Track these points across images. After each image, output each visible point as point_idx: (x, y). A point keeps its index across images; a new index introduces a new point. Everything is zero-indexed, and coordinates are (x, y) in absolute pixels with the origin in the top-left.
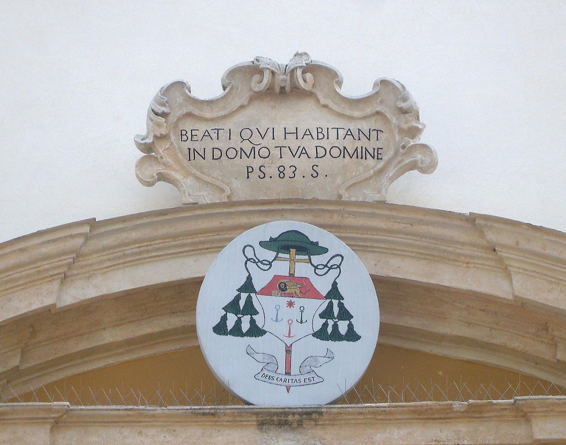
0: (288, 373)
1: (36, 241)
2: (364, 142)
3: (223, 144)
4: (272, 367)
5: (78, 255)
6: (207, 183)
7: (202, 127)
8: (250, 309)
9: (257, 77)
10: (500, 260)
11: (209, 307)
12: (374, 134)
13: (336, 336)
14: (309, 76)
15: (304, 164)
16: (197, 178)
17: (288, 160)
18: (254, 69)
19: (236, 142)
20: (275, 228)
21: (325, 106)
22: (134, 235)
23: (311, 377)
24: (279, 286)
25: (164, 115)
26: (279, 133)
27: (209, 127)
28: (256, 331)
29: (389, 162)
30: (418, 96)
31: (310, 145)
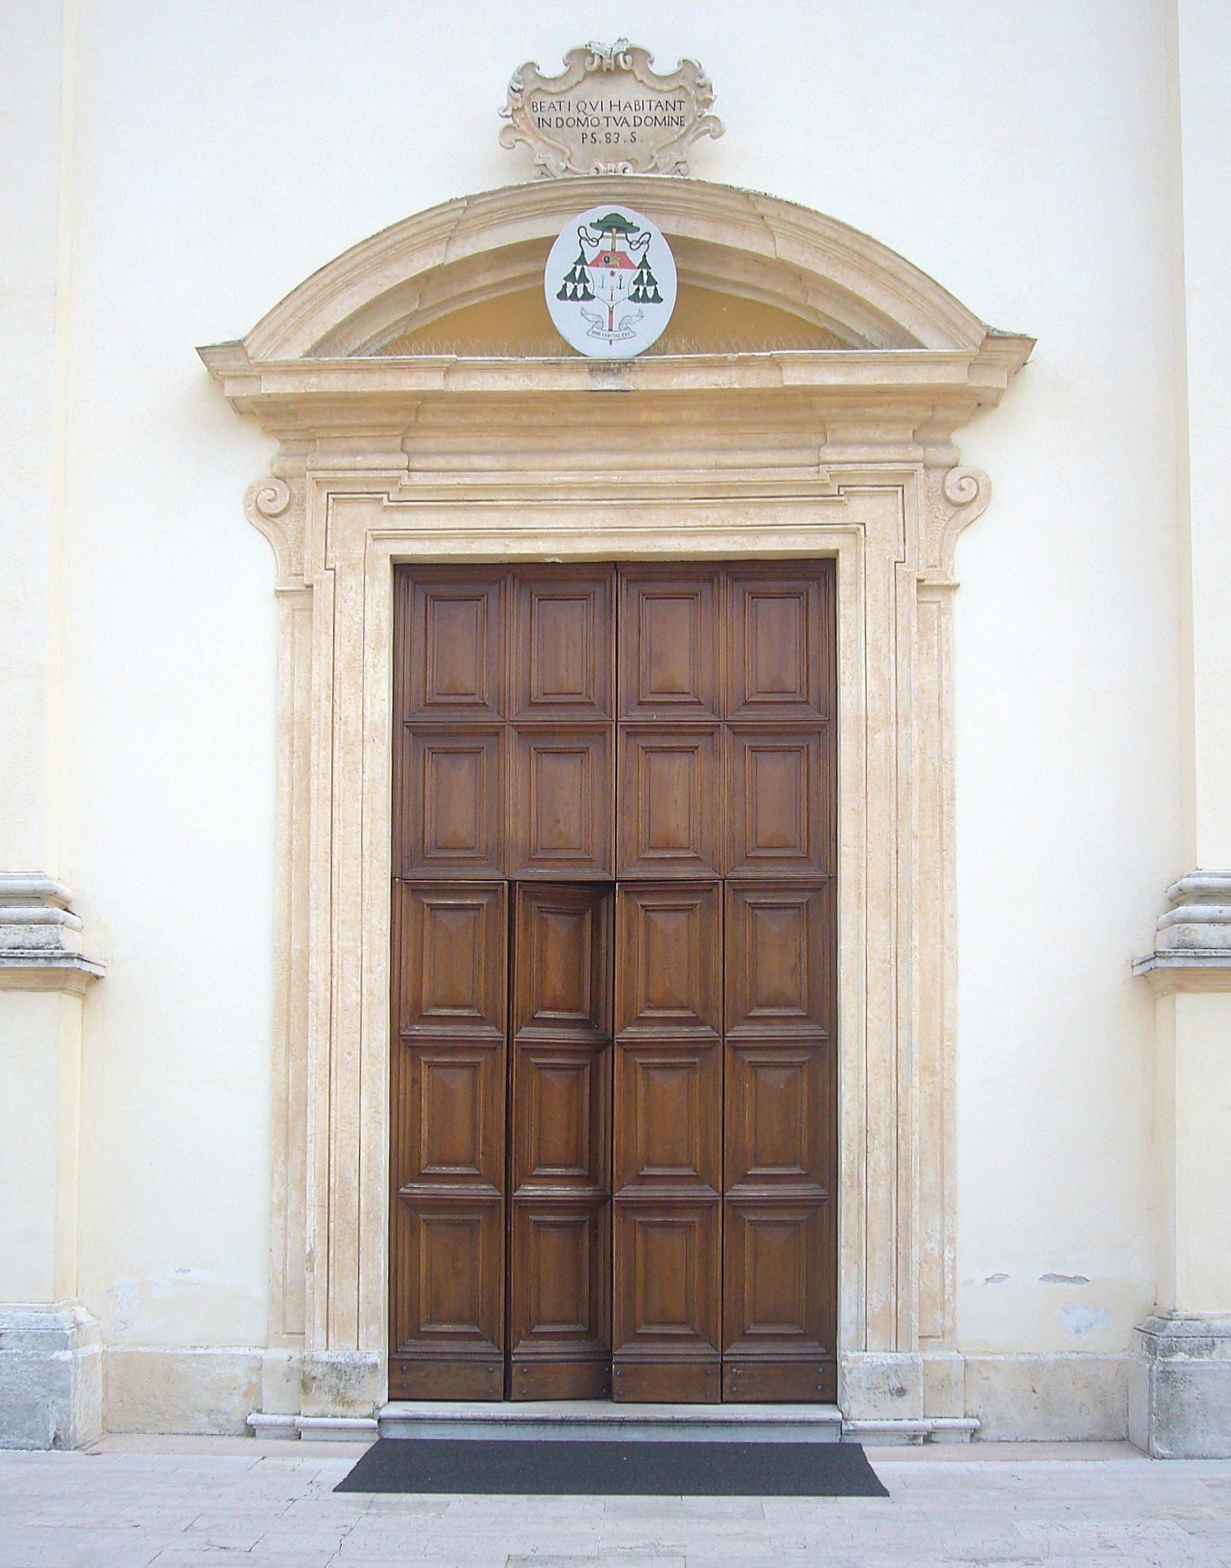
0: (611, 330)
1: (429, 215)
2: (670, 112)
3: (564, 115)
4: (600, 325)
5: (459, 221)
6: (554, 147)
7: (548, 100)
8: (584, 279)
9: (589, 59)
10: (768, 226)
11: (553, 281)
12: (678, 104)
13: (645, 299)
14: (628, 58)
15: (625, 132)
16: (545, 142)
17: (613, 128)
18: (586, 53)
19: (574, 114)
20: (601, 212)
21: (641, 81)
22: (499, 204)
23: (629, 334)
24: (604, 259)
25: (520, 91)
26: (606, 106)
27: (554, 99)
28: (588, 296)
29: (690, 127)
30: (712, 74)
31: (630, 115)
